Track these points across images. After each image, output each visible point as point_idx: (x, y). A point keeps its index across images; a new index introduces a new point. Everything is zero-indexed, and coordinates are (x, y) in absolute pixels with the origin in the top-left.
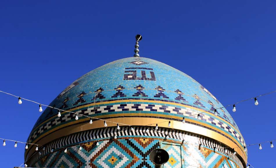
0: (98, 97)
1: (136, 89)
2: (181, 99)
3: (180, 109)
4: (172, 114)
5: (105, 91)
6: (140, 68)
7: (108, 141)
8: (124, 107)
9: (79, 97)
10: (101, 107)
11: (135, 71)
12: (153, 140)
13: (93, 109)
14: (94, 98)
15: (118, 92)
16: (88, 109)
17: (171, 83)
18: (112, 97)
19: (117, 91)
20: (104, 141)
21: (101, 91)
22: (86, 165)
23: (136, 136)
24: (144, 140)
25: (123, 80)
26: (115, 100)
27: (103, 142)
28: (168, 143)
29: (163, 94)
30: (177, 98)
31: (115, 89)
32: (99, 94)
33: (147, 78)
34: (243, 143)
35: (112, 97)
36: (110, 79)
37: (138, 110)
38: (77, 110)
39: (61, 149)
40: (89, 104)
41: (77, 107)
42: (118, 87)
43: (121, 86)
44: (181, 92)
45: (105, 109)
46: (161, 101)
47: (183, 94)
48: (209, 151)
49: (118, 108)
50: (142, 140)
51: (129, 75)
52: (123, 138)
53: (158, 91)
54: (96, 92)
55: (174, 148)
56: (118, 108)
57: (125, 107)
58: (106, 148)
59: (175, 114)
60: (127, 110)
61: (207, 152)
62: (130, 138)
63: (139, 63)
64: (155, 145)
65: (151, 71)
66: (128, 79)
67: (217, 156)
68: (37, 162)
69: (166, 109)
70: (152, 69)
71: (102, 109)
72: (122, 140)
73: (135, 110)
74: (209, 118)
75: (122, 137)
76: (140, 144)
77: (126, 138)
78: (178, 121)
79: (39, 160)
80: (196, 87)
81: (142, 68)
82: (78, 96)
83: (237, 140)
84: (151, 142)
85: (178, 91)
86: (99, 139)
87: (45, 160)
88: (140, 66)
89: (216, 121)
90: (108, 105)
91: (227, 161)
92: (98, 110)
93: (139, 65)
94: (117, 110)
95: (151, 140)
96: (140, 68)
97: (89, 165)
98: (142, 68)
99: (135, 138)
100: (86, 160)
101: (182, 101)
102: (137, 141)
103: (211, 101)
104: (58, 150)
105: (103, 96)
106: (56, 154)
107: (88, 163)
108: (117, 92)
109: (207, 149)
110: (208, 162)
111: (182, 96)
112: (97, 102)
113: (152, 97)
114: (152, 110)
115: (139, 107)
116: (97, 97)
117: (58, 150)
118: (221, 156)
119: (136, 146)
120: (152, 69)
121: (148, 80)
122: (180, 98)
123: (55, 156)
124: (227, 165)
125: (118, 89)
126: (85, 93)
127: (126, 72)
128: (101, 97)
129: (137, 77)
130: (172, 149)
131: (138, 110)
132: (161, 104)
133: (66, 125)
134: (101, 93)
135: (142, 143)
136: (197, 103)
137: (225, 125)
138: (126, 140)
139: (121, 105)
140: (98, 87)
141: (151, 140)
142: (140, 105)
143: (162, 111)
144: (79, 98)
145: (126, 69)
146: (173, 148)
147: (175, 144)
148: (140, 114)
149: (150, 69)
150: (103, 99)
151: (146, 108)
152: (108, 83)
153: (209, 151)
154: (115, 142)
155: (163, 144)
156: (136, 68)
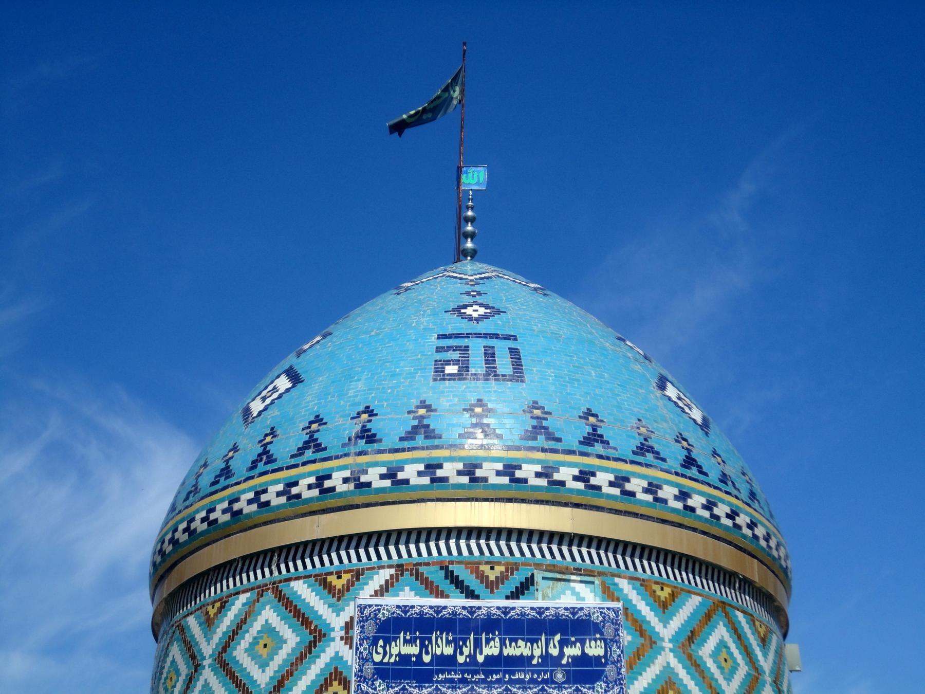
0: (362, 438)
1: (470, 412)
2: (598, 442)
3: (594, 474)
4: (571, 491)
5: (381, 420)
6: (479, 336)
7: (393, 571)
8: (435, 473)
9: (308, 431)
10: (370, 470)
11: (467, 348)
12: (517, 569)
13: (347, 474)
14: (350, 439)
15: (419, 422)
16: (334, 475)
17: (569, 390)
18: (401, 439)
19: (414, 418)
20: (381, 571)
21: (370, 416)
22: (333, 640)
23: (471, 559)
24: (492, 568)
25: (431, 383)
26: (410, 449)
27: (378, 574)
28: (558, 576)
29: (546, 428)
30: (584, 438)
31: (409, 412)
32: (364, 430)
33: (498, 375)
34: (777, 550)
35: (401, 439)
36: (394, 375)
37: (474, 480)
38: (304, 476)
39: (259, 587)
40: (337, 457)
41: (304, 464)
42: (418, 407)
43: (425, 401)
44: (596, 416)
45: (383, 477)
46: (538, 451)
47: (602, 424)
48: (675, 590)
49: (420, 474)
50: (485, 568)
51: (448, 363)
52: (434, 564)
53: (532, 417)
54: (355, 421)
55: (574, 588)
56: (420, 474)
57: (439, 473)
58: (387, 591)
59: (578, 492)
60: (444, 480)
61: (667, 596)
62: (452, 563)
63: (475, 315)
64: (521, 583)
65: (512, 344)
66: (444, 379)
67: (698, 604)
68: (192, 613)
69: (552, 476)
70: (514, 338)
71: (373, 476)
72: (432, 568)
73: (465, 479)
74: (677, 493)
75: (430, 560)
76: (482, 582)
77: (442, 562)
78: (586, 509)
79: (198, 610)
80: (641, 391)
81: (485, 336)
82: (303, 429)
83: (758, 545)
84: (512, 574)
85: (589, 413)
86: (365, 564)
87: (215, 614)
88: (482, 327)
89: (696, 501)
90: (390, 466)
91: (727, 615)
92: (364, 479)
93: (478, 320)
94: (415, 481)
95: (512, 568)
96: (479, 336)
97: (342, 638)
98: (485, 336)
99: (467, 564)
100: (332, 626)
101: (598, 448)
102: (471, 573)
103: (685, 435)
104: (253, 589)
105: (375, 435)
106: (247, 598)
107: (338, 633)
108: (416, 423)
109: (668, 586)
110: (669, 623)
111: (599, 431)
112: (360, 454)
114: (514, 480)
115: (479, 473)
116: (358, 437)
117: (253, 589)
118: (710, 602)
119: (471, 588)
120: (514, 338)
121: (504, 380)
122: (594, 437)
123: (244, 605)
124: (724, 625)
125: (417, 415)
126: (322, 419)
127: (439, 349)
128: (367, 436)
129: (472, 371)
130: (568, 592)
131: (474, 480)
132: (538, 462)
134: (369, 426)
135: (487, 577)
136: (644, 449)
137: (721, 510)
138: (441, 568)
139: (428, 466)
140: (359, 404)
141: (512, 568)
142: (479, 466)
143: (543, 482)
144: (307, 434)
145: (441, 337)
146: (573, 589)
147: (579, 578)
148: (479, 491)
149: (507, 338)
150: (376, 446)
151: (499, 473)
152: (389, 391)
153: (673, 592)
154: (412, 575)
155: (544, 578)
156: (468, 336)
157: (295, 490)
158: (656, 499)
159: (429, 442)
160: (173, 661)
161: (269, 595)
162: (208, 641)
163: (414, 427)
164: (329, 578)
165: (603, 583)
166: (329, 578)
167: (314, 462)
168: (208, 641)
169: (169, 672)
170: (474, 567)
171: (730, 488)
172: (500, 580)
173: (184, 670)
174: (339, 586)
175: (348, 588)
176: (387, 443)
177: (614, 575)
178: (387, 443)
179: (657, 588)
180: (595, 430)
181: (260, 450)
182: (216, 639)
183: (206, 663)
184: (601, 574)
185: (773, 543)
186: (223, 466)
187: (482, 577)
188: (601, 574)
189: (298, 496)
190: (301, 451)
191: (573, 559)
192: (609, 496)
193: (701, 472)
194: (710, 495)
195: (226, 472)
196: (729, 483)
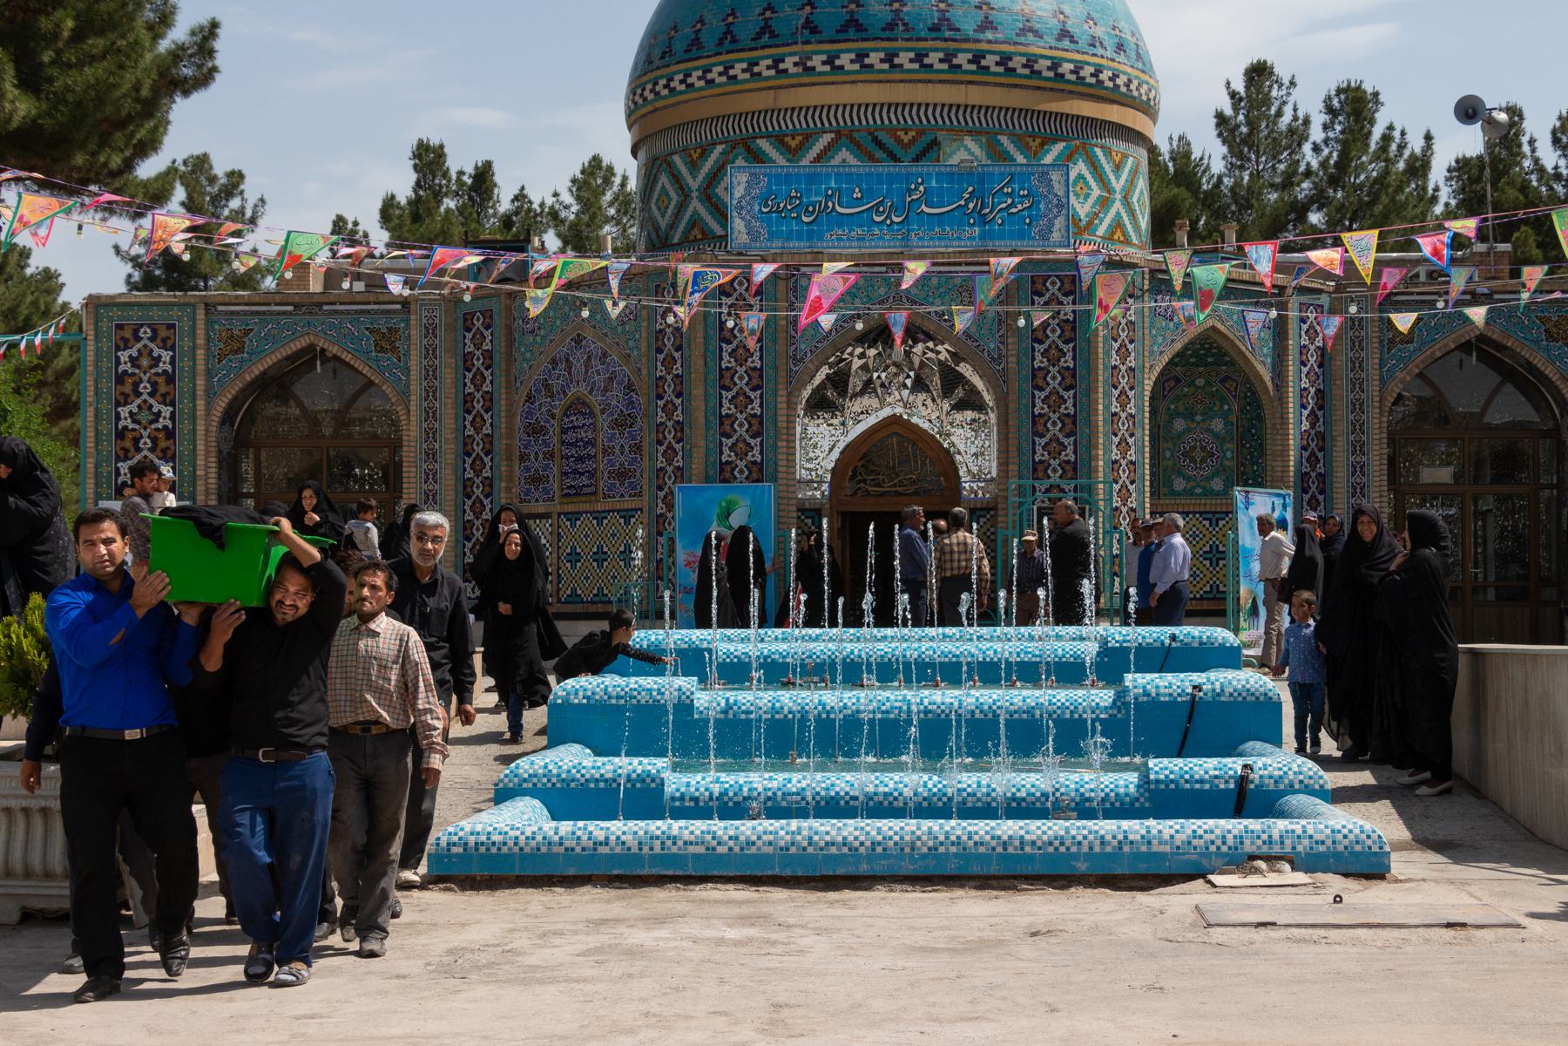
7: (833, 135)
13: (796, 59)
16: (787, 59)
18: (837, 31)
29: (948, 20)
32: (808, 21)
35: (837, 31)
37: (893, 66)
41: (763, 48)
57: (867, 61)
91: (1087, 153)
94: (848, 67)
108: (848, 17)
113: (923, 34)
114: (923, 66)
131: (893, 66)
133: (738, 87)
139: (857, 55)
141: (921, 133)
151: (911, 61)
157: (756, 69)
158: (1033, 72)
159: (860, 35)
160: (663, 187)
161: (740, 149)
162: (694, 178)
163: (847, 21)
164: (786, 139)
165: (988, 141)
166: (786, 139)
167: (771, 46)
168: (694, 178)
169: (660, 195)
170: (892, 132)
171: (1100, 51)
172: (913, 141)
173: (675, 197)
174: (793, 146)
175: (801, 146)
176: (829, 33)
177: (997, 134)
178: (825, 36)
179: (1030, 140)
180: (986, 18)
181: (724, 29)
182: (700, 177)
183: (695, 194)
184: (986, 133)
185: (1133, 87)
186: (693, 36)
187: (899, 141)
188: (986, 133)
189: (759, 74)
190: (759, 36)
191: (967, 124)
192: (996, 74)
193: (1073, 41)
194: (1076, 61)
195: (696, 42)
196: (1097, 44)
